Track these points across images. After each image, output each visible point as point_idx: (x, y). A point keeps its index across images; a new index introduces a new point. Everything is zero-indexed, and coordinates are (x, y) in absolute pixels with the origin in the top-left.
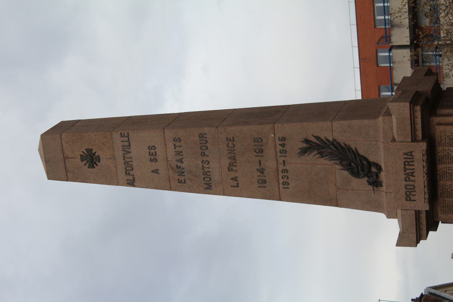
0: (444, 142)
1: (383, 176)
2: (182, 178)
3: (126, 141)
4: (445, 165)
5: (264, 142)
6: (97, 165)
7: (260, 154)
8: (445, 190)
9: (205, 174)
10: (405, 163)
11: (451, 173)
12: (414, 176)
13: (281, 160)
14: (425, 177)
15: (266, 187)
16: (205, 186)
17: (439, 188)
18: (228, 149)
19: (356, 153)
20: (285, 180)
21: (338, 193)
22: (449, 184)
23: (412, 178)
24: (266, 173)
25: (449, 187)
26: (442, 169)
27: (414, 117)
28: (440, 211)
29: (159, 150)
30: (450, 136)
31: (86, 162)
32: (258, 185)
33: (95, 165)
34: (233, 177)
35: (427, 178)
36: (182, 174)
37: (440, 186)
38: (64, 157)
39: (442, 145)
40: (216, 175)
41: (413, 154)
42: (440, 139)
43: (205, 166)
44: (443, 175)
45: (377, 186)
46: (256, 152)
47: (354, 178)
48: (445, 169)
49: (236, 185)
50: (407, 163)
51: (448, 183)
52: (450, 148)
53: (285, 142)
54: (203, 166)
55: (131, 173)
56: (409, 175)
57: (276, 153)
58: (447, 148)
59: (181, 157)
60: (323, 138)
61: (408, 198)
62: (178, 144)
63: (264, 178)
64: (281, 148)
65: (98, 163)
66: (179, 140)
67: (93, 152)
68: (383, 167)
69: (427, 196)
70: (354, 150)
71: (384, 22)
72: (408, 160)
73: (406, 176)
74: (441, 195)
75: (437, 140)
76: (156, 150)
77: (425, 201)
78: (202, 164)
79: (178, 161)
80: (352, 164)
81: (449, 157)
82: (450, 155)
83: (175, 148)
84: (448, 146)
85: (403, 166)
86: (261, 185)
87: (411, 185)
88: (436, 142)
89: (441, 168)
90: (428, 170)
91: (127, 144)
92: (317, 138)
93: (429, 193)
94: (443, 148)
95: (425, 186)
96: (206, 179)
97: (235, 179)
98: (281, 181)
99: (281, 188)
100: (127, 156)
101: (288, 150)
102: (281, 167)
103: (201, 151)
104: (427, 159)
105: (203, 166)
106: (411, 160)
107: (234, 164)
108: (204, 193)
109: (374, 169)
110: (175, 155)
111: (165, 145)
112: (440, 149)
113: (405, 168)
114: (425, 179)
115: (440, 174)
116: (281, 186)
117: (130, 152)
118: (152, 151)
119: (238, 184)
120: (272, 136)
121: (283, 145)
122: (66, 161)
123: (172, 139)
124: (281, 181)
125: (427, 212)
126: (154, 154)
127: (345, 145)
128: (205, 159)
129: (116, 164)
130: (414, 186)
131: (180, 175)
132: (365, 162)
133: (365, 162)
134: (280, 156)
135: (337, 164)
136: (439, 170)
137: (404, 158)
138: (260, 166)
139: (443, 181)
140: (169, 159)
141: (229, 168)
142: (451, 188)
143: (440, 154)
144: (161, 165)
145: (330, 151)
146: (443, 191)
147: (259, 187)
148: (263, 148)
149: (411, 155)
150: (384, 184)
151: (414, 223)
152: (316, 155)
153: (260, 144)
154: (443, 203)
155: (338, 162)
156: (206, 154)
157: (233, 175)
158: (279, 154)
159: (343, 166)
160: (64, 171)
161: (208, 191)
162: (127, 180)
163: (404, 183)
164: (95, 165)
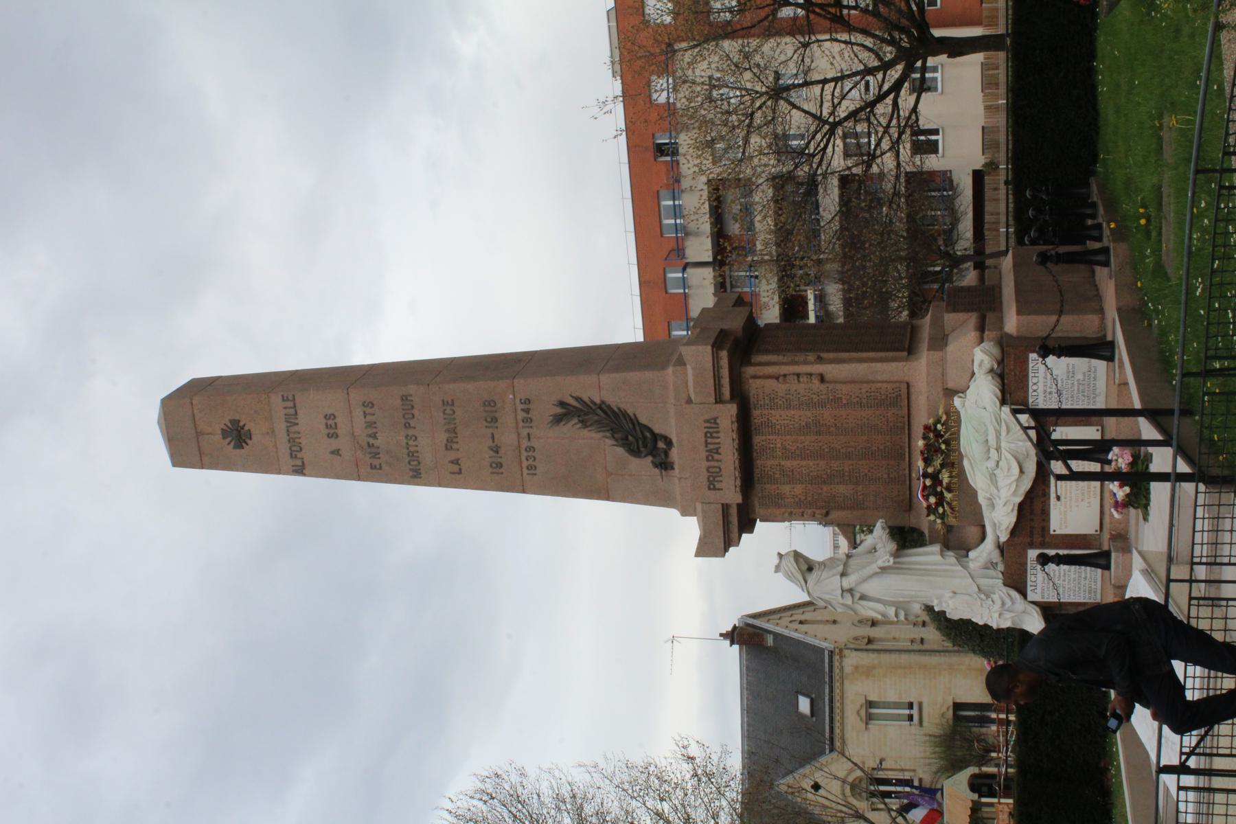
1: (675, 454)
2: (376, 462)
3: (291, 408)
4: (764, 437)
5: (499, 405)
6: (247, 444)
7: (492, 424)
9: (411, 455)
10: (706, 433)
12: (720, 454)
13: (524, 432)
14: (736, 454)
15: (502, 473)
16: (411, 473)
17: (757, 471)
18: (445, 416)
19: (634, 421)
21: (609, 480)
23: (716, 456)
24: (502, 451)
27: (718, 367)
31: (230, 439)
32: (491, 470)
33: (244, 444)
34: (452, 459)
36: (375, 455)
38: (196, 432)
40: (427, 457)
41: (718, 421)
43: (411, 442)
45: (666, 469)
46: (486, 420)
47: (632, 459)
49: (457, 470)
50: (709, 435)
51: (769, 463)
53: (531, 406)
54: (407, 444)
55: (299, 455)
56: (713, 453)
57: (517, 423)
58: (766, 412)
59: (374, 430)
60: (586, 400)
61: (712, 487)
62: (368, 410)
63: (499, 460)
64: (524, 415)
65: (249, 442)
66: (370, 405)
67: (241, 424)
68: (674, 440)
69: (738, 482)
70: (633, 417)
71: (674, 227)
72: (711, 430)
73: (707, 454)
75: (752, 400)
76: (336, 421)
78: (405, 441)
79: (370, 436)
80: (630, 438)
83: (365, 417)
85: (703, 439)
86: (495, 470)
87: (717, 467)
90: (739, 444)
91: (292, 411)
92: (578, 399)
95: (735, 468)
96: (412, 463)
97: (456, 462)
98: (525, 464)
101: (534, 418)
102: (525, 443)
103: (403, 421)
104: (738, 429)
105: (407, 444)
106: (715, 430)
107: (454, 440)
108: (409, 483)
109: (661, 445)
110: (366, 428)
111: (351, 412)
112: (756, 413)
113: (706, 441)
116: (525, 471)
117: (297, 424)
118: (330, 422)
119: (460, 469)
120: (511, 396)
121: (527, 411)
122: (200, 438)
123: (361, 403)
124: (525, 464)
125: (738, 505)
126: (333, 426)
127: (619, 409)
128: (411, 432)
129: (275, 442)
130: (720, 468)
132: (648, 435)
133: (648, 435)
134: (523, 427)
135: (607, 437)
137: (705, 428)
138: (493, 442)
140: (356, 434)
141: (446, 445)
143: (756, 421)
144: (343, 443)
145: (596, 418)
147: (492, 473)
148: (497, 415)
149: (715, 423)
150: (676, 466)
151: (721, 523)
152: (575, 424)
153: (494, 409)
155: (608, 434)
156: (412, 425)
157: (452, 455)
158: (521, 424)
159: (616, 440)
160: (198, 453)
161: (416, 480)
162: (293, 466)
163: (705, 464)
164: (244, 444)
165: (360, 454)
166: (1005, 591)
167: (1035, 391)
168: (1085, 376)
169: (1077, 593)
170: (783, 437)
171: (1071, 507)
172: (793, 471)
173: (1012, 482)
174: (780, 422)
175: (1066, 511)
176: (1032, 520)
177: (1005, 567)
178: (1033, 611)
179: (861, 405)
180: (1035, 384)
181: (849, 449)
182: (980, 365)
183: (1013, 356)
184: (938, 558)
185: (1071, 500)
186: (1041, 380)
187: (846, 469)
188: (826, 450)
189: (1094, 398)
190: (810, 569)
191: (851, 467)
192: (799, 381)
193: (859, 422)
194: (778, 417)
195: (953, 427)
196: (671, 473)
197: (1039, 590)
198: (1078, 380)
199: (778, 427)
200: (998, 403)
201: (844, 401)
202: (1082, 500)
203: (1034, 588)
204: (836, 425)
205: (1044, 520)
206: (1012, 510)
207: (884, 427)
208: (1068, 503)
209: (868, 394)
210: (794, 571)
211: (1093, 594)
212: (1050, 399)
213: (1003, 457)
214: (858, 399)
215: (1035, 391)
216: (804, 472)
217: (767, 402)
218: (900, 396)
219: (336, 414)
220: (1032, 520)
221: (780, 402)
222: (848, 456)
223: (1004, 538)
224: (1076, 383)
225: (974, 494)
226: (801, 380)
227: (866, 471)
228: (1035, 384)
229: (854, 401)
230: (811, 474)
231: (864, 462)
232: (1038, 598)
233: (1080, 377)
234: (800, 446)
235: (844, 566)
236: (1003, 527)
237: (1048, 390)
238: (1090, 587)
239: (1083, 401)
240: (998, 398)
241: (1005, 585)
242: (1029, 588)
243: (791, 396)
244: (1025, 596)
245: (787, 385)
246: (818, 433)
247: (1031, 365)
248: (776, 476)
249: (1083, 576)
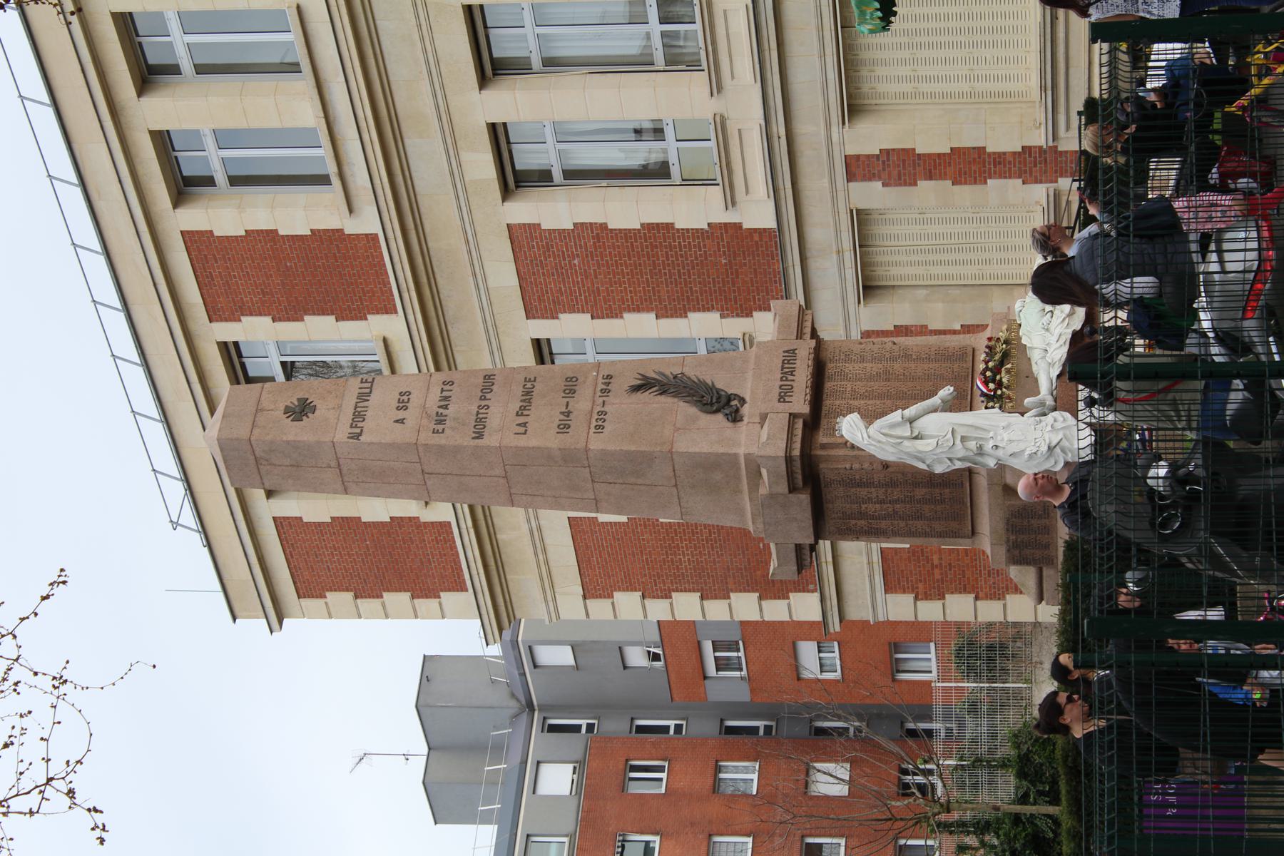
1: (745, 410)
2: (440, 427)
7: (570, 395)
14: (809, 377)
20: (600, 423)
21: (675, 434)
23: (790, 377)
24: (572, 416)
29: (415, 400)
41: (796, 352)
59: (447, 403)
65: (310, 415)
67: (308, 402)
68: (747, 399)
69: (808, 397)
85: (780, 365)
99: (591, 433)
100: (359, 405)
102: (599, 408)
113: (782, 366)
119: (526, 430)
120: (595, 374)
127: (697, 377)
128: (483, 403)
131: (439, 424)
150: (746, 419)
157: (522, 419)
158: (600, 394)
165: (425, 422)
170: (855, 384)
179: (929, 359)
196: (739, 424)
201: (914, 357)
206: (1065, 343)
219: (412, 391)
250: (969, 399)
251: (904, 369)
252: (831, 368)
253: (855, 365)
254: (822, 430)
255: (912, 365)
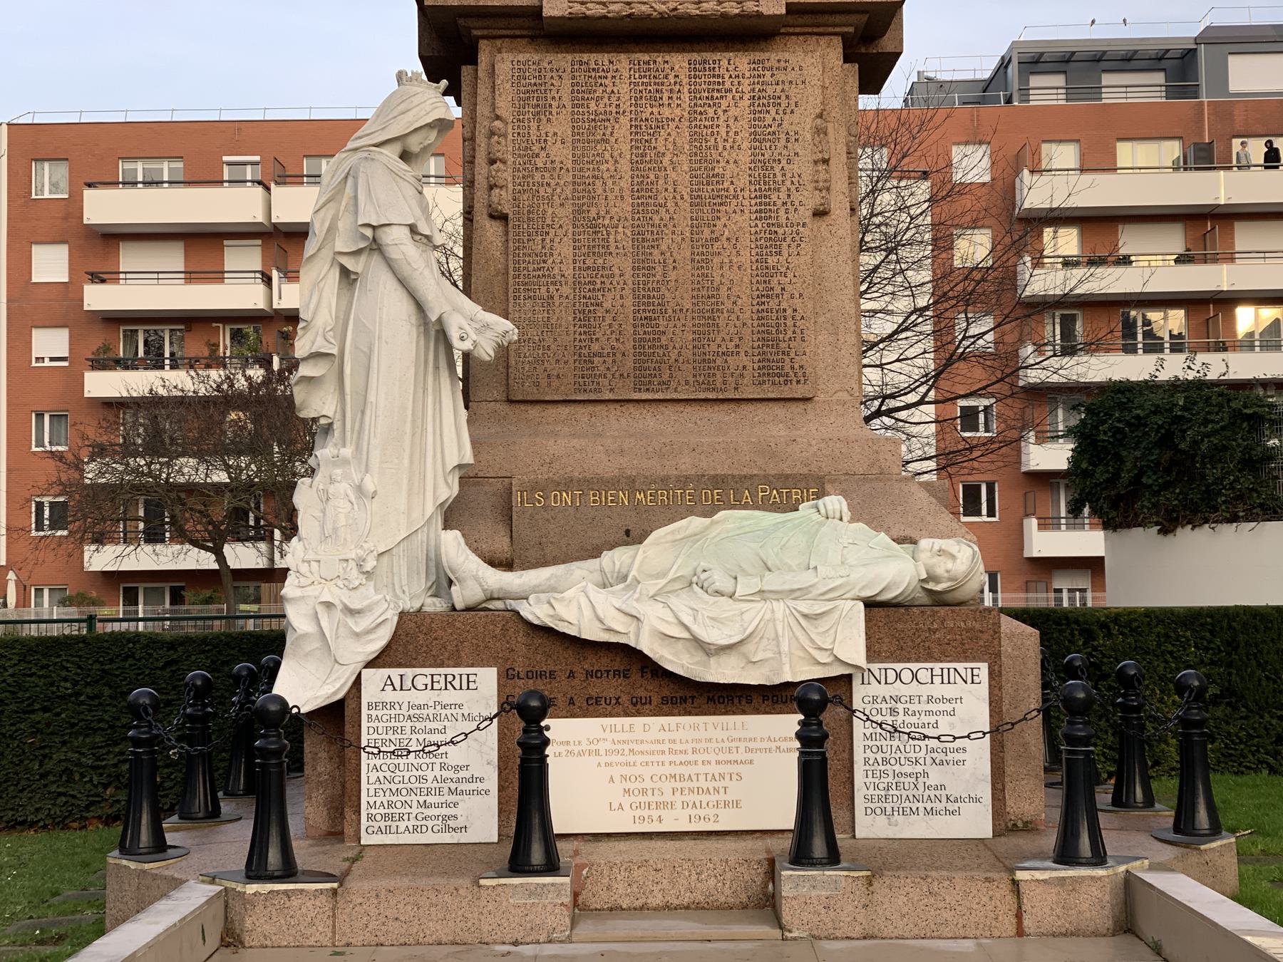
0: (768, 78)
4: (686, 80)
8: (600, 77)
11: (661, 98)
14: (663, 8)
17: (603, 59)
22: (621, 91)
25: (609, 90)
26: (672, 69)
28: (521, 57)
30: (787, 97)
35: (660, 13)
37: (611, 62)
39: (756, 73)
42: (777, 65)
44: (653, 73)
48: (672, 81)
51: (624, 88)
52: (746, 96)
58: (746, 87)
74: (581, 63)
77: (576, 4)
81: (715, 95)
82: (722, 97)
84: (753, 90)
88: (767, 55)
89: (677, 67)
90: (690, 17)
93: (605, 17)
94: (747, 75)
104: (724, 16)
114: (654, 5)
115: (655, 62)
136: (667, 58)
139: (632, 72)
142: (607, 95)
143: (724, 63)
146: (594, 70)
154: (552, 70)
166: (389, 615)
167: (898, 676)
168: (936, 788)
169: (387, 786)
171: (608, 764)
172: (607, 141)
173: (687, 628)
174: (723, 118)
175: (597, 752)
176: (572, 675)
177: (429, 614)
178: (338, 685)
180: (915, 676)
181: (659, 269)
182: (941, 552)
183: (978, 626)
184: (453, 461)
185: (628, 764)
186: (925, 691)
187: (611, 260)
188: (656, 219)
189: (884, 811)
190: (405, 156)
191: (617, 272)
192: (816, 162)
193: (724, 289)
194: (733, 112)
195: (753, 495)
197: (390, 695)
198: (926, 774)
199: (711, 112)
200: (868, 593)
201: (772, 261)
202: (627, 791)
203: (397, 685)
204: (717, 239)
205: (572, 702)
206: (609, 630)
207: (714, 347)
208: (619, 758)
209: (789, 312)
210: (411, 114)
211: (383, 824)
212: (879, 711)
213: (744, 606)
214: (778, 290)
215: (898, 676)
216: (604, 167)
217: (770, 90)
218: (786, 383)
220: (572, 675)
221: (769, 120)
222: (642, 266)
223: (535, 612)
224: (919, 769)
225: (632, 537)
226: (821, 167)
227: (607, 305)
228: (915, 676)
229: (774, 281)
230: (599, 183)
231: (629, 302)
232: (369, 693)
233: (936, 775)
234: (666, 161)
235: (427, 237)
236: (562, 610)
237: (900, 707)
238: (401, 818)
239: (876, 787)
240: (896, 597)
241: (402, 615)
242: (395, 673)
243: (783, 142)
244: (370, 664)
245: (809, 136)
246: (697, 201)
247: (960, 666)
248: (592, 104)
249: (430, 799)
250: (637, 396)
251: (734, 241)
252: (735, 64)
253: (744, 123)
254: (536, 57)
255: (746, 258)
